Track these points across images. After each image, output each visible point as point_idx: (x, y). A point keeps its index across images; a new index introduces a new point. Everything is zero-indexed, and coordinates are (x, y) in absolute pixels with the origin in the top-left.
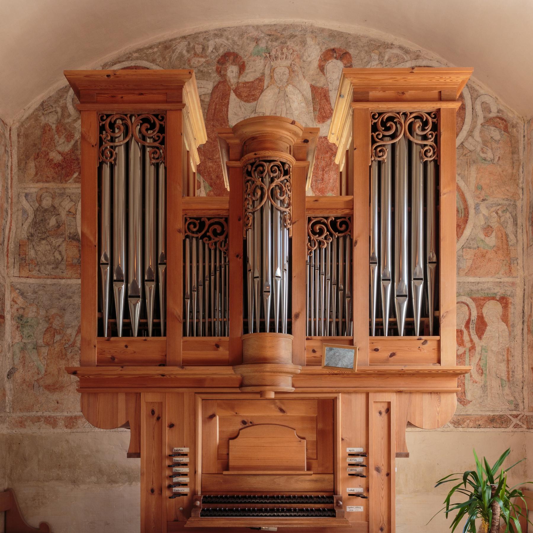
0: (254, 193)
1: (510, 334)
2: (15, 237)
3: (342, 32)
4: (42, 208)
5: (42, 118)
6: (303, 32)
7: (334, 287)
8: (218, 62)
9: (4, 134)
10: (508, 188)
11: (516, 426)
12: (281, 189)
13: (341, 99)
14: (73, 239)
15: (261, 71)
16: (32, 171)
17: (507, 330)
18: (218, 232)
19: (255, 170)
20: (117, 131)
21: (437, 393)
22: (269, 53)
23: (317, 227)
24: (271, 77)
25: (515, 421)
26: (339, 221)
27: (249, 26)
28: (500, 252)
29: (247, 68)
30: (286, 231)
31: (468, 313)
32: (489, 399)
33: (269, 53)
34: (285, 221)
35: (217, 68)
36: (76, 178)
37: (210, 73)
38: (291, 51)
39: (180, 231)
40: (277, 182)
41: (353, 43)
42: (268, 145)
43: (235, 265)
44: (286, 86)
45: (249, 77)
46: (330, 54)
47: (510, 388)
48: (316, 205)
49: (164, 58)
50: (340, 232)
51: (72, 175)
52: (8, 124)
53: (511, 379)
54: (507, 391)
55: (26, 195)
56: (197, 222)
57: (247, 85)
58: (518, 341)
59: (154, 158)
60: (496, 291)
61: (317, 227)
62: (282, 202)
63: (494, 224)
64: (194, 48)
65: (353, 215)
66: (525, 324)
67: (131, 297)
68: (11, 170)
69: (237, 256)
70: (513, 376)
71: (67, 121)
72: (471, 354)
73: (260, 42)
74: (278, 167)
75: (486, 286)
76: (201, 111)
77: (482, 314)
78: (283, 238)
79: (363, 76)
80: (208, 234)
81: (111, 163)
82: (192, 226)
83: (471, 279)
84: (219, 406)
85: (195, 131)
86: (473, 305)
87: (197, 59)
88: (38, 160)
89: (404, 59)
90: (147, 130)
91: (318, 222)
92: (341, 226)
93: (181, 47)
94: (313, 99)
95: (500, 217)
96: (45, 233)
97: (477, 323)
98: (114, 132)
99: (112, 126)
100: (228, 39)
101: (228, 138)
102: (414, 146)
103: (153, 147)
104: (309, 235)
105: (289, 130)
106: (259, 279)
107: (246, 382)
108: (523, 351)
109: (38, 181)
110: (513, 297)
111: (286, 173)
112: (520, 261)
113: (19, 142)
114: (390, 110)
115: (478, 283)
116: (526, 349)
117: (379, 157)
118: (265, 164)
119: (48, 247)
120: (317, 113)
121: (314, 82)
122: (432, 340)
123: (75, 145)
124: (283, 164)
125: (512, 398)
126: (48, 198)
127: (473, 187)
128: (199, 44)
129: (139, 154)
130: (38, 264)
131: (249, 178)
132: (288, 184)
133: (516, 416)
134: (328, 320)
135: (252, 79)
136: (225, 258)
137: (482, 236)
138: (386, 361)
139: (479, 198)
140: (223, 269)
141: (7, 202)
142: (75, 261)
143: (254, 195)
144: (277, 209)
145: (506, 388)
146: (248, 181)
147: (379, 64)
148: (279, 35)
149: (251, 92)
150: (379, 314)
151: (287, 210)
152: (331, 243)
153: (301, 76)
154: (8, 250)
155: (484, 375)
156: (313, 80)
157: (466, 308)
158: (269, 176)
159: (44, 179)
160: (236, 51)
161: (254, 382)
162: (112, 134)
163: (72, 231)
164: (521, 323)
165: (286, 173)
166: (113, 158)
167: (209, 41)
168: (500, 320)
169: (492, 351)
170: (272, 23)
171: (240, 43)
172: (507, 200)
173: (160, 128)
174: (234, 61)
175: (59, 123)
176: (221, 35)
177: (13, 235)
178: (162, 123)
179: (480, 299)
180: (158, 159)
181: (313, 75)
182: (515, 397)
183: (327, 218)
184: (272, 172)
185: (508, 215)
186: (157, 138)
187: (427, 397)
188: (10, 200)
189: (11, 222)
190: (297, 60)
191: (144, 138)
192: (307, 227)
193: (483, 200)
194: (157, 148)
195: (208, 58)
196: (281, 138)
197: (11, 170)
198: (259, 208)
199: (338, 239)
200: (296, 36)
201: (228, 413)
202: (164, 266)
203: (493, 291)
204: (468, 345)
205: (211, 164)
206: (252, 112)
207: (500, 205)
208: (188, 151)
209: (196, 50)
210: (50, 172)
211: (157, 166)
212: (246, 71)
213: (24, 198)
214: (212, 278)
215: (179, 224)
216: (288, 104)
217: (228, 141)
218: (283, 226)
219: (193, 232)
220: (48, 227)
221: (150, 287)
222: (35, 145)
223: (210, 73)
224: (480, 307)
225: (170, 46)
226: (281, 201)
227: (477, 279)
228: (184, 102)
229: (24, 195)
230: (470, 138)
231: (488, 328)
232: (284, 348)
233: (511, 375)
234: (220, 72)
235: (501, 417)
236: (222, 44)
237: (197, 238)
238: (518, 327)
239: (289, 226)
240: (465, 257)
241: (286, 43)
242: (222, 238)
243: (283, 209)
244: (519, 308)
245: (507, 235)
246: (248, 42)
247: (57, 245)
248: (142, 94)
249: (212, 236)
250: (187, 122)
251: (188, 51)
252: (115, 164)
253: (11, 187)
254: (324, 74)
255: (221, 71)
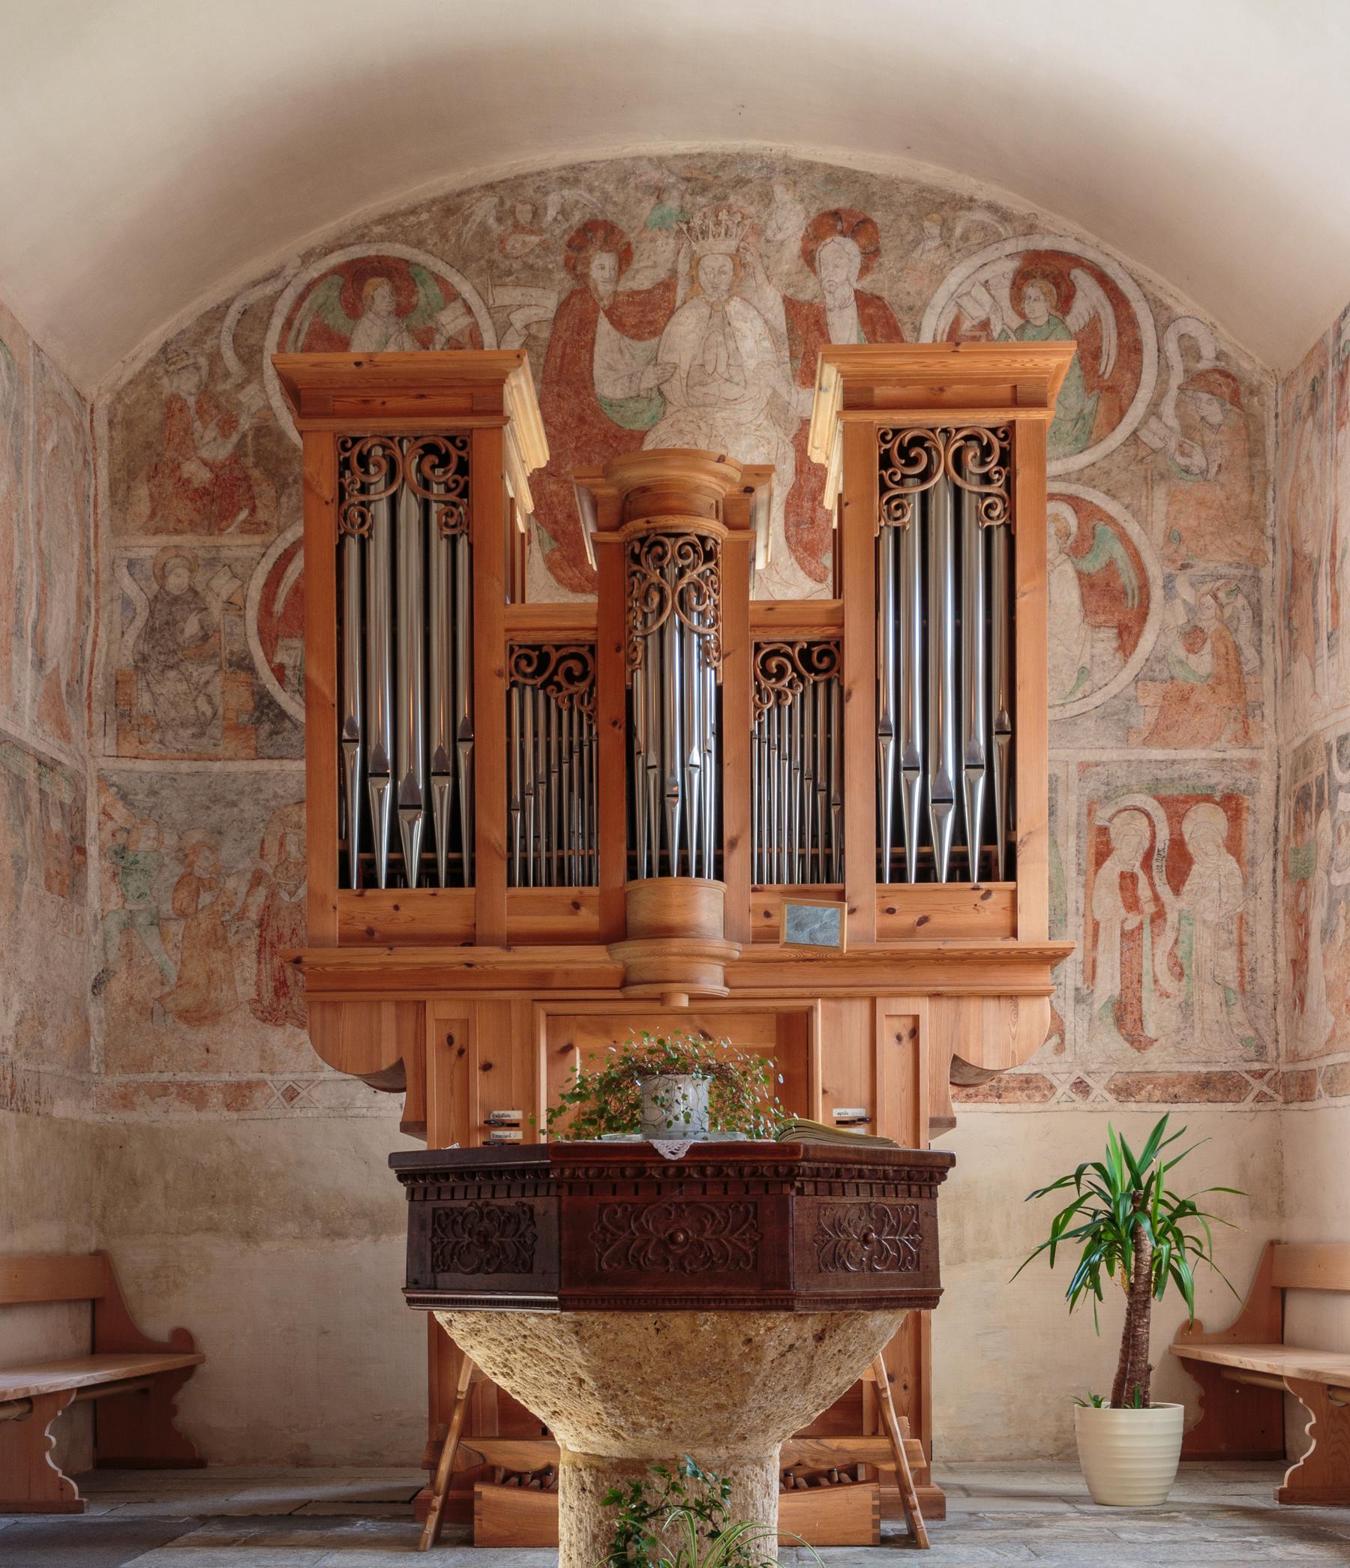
0: (645, 599)
1: (1245, 883)
2: (107, 664)
3: (855, 172)
4: (168, 594)
5: (165, 381)
6: (765, 171)
7: (809, 785)
8: (570, 245)
9: (81, 424)
10: (1239, 538)
11: (1261, 1097)
12: (699, 589)
13: (822, 394)
14: (239, 666)
15: (669, 266)
16: (144, 508)
17: (1238, 872)
18: (577, 674)
19: (648, 552)
20: (372, 469)
21: (1013, 997)
22: (688, 223)
23: (773, 663)
24: (693, 280)
25: (1258, 1086)
26: (816, 649)
27: (640, 158)
28: (1223, 689)
29: (636, 257)
30: (710, 673)
31: (1148, 834)
32: (1197, 1034)
33: (688, 223)
34: (707, 653)
35: (566, 264)
36: (244, 522)
37: (550, 272)
38: (738, 218)
39: (500, 674)
40: (691, 575)
41: (881, 197)
42: (674, 503)
43: (611, 741)
44: (727, 301)
45: (642, 279)
46: (828, 223)
47: (1245, 1009)
48: (772, 618)
49: (444, 237)
50: (817, 672)
51: (235, 515)
52: (88, 398)
53: (1248, 987)
54: (1238, 1015)
55: (131, 564)
56: (534, 654)
57: (637, 299)
58: (1265, 899)
59: (446, 524)
60: (1213, 781)
61: (773, 663)
62: (702, 614)
63: (1209, 623)
64: (512, 212)
65: (843, 637)
66: (1280, 858)
67: (403, 807)
68: (95, 506)
69: (614, 724)
70: (1254, 980)
71: (222, 387)
72: (1156, 931)
73: (665, 196)
74: (693, 546)
75: (1190, 769)
76: (538, 412)
77: (1181, 835)
78: (704, 683)
79: (860, 360)
80: (556, 678)
81: (362, 536)
82: (523, 663)
83: (1157, 754)
84: (582, 1028)
85: (527, 444)
86: (1159, 815)
87: (520, 237)
88: (156, 481)
89: (1000, 235)
90: (433, 467)
91: (775, 653)
92: (820, 660)
93: (484, 210)
94: (790, 330)
95: (1221, 606)
96: (175, 652)
97: (1170, 857)
98: (367, 472)
99: (364, 460)
100: (591, 190)
101: (596, 486)
102: (966, 497)
103: (445, 503)
104: (756, 679)
105: (715, 474)
106: (656, 771)
107: (634, 976)
108: (1275, 922)
109: (157, 531)
110: (1252, 794)
111: (709, 556)
112: (1268, 710)
113: (111, 438)
114: (916, 424)
115: (1173, 762)
116: (1280, 915)
117: (896, 519)
118: (666, 540)
119: (182, 687)
120: (798, 364)
121: (791, 291)
122: (1000, 888)
123: (241, 444)
124: (703, 539)
125: (1251, 1033)
126: (180, 571)
127: (1159, 537)
128: (523, 202)
129: (416, 513)
130: (158, 726)
131: (636, 567)
132: (713, 578)
133: (1261, 1075)
134: (797, 851)
135: (647, 285)
136: (590, 727)
137: (1182, 653)
138: (909, 933)
139: (1174, 561)
140: (586, 749)
141: (89, 581)
142: (245, 718)
143: (646, 603)
144: (692, 631)
145: (1237, 1008)
146: (634, 574)
147: (940, 246)
148: (710, 178)
149: (646, 315)
150: (898, 839)
151: (712, 631)
152: (802, 694)
153: (761, 277)
154: (90, 695)
155: (1185, 978)
156: (789, 286)
157: (1145, 821)
158: (676, 564)
159: (171, 526)
160: (610, 218)
161: (647, 975)
162: (364, 478)
163: (236, 647)
164: (1270, 856)
165: (709, 556)
166: (366, 527)
167: (547, 194)
168: (1224, 850)
169: (1204, 921)
170: (694, 151)
171: (619, 198)
172: (1239, 565)
173: (458, 460)
174: (605, 240)
175: (205, 393)
176: (577, 181)
177: (100, 657)
178: (462, 453)
179: (1178, 801)
180: (454, 527)
181: (788, 274)
182: (1256, 1030)
183: (792, 644)
184: (681, 556)
185: (1241, 601)
186: (453, 486)
187: (991, 1005)
188: (93, 577)
189: (96, 628)
190: (752, 239)
191: (426, 485)
192: (752, 663)
193: (1184, 567)
194: (454, 504)
195: (547, 236)
196: (698, 489)
197: (95, 506)
198: (656, 628)
199: (815, 685)
200: (749, 181)
201: (596, 1043)
202: (470, 745)
203: (1206, 781)
204: (1149, 908)
205: (554, 487)
206: (648, 363)
207: (1221, 577)
208: (512, 499)
209: (519, 216)
210: (183, 509)
211: (453, 541)
212: (635, 266)
213: (125, 570)
214: (565, 767)
215: (497, 659)
216: (731, 344)
217: (595, 491)
218: (704, 664)
219: (525, 675)
220: (180, 640)
221: (442, 786)
222: (149, 446)
223: (550, 272)
224: (1176, 818)
225: (458, 208)
226: (699, 613)
227: (1170, 754)
228: (507, 413)
229: (125, 563)
230: (1153, 420)
231: (1195, 867)
232: (707, 906)
233: (1247, 979)
234: (574, 268)
235: (1224, 1076)
236: (577, 202)
237: (533, 687)
238: (1264, 865)
239: (715, 664)
240: (1141, 702)
241: (725, 198)
242: (583, 686)
243: (701, 629)
244: (1267, 820)
245: (1238, 649)
246: (639, 195)
247: (203, 680)
248: (422, 396)
249: (564, 684)
250: (510, 444)
251: (499, 220)
252: (370, 536)
253: (96, 546)
254: (814, 271)
255: (576, 267)
